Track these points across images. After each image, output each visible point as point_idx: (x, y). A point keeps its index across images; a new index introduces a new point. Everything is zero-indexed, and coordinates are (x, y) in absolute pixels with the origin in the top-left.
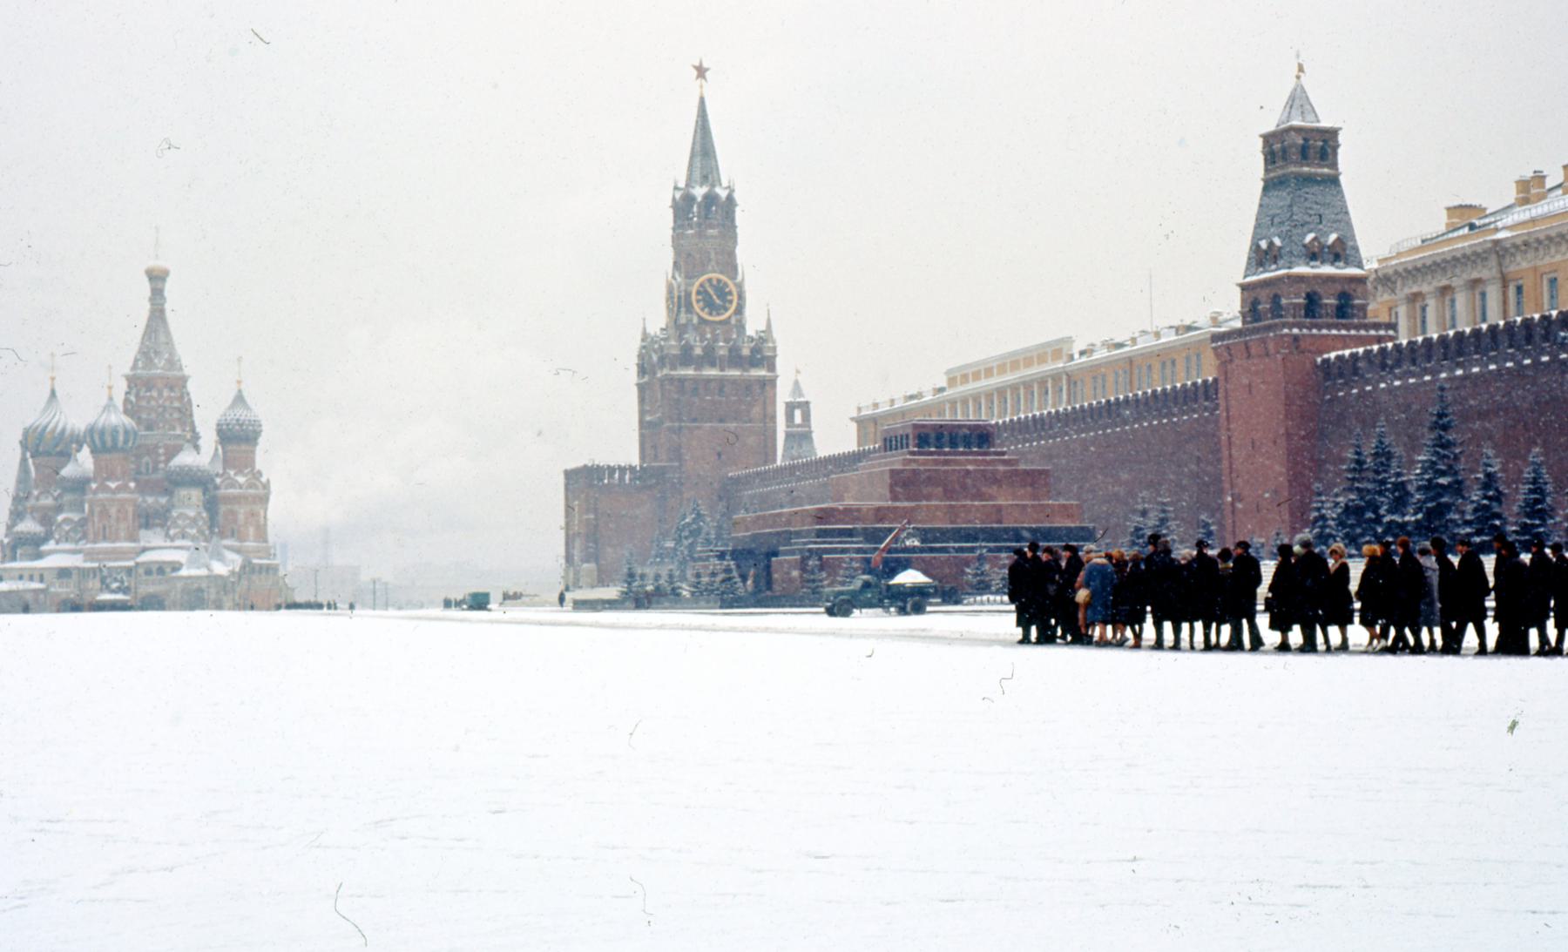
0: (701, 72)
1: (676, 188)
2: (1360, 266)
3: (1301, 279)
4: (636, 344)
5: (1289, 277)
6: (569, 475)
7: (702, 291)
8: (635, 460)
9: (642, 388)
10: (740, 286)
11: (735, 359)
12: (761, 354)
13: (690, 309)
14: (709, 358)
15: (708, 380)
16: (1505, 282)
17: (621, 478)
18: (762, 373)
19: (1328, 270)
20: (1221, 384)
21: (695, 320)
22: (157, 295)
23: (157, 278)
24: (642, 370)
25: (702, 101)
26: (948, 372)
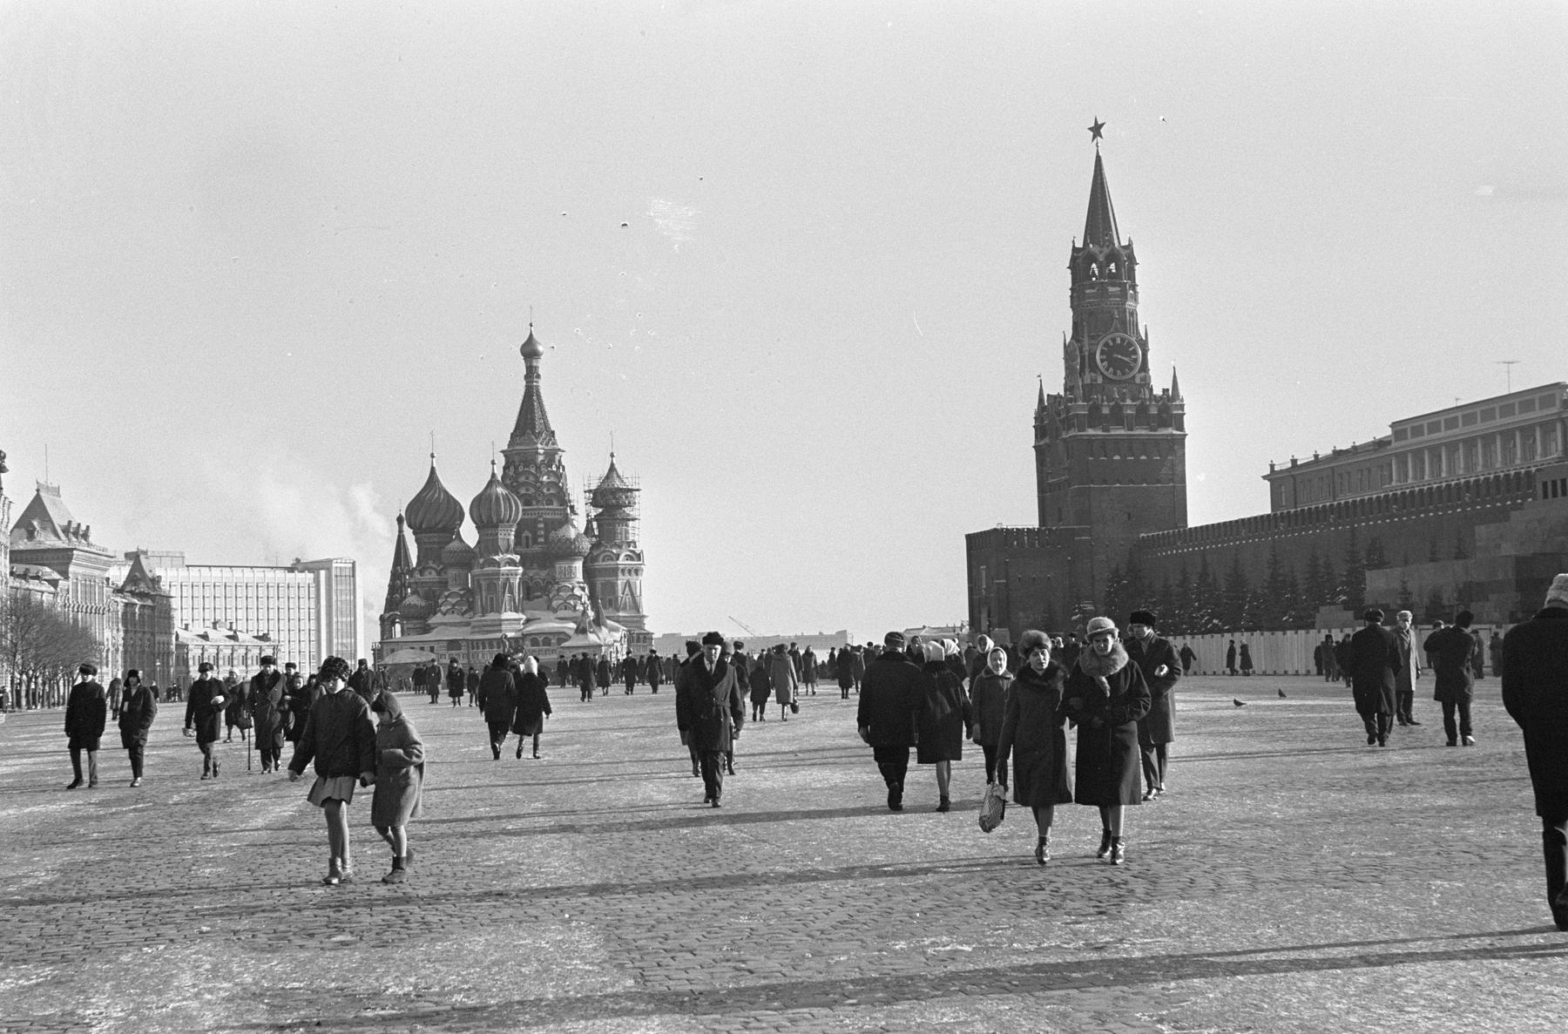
0: (1096, 130)
1: (1075, 249)
6: (971, 539)
7: (1108, 352)
10: (1144, 344)
11: (1142, 416)
12: (1168, 411)
14: (1117, 417)
15: (1117, 440)
21: (1100, 380)
22: (531, 374)
23: (530, 352)
24: (1041, 430)
25: (1098, 159)
26: (1393, 425)
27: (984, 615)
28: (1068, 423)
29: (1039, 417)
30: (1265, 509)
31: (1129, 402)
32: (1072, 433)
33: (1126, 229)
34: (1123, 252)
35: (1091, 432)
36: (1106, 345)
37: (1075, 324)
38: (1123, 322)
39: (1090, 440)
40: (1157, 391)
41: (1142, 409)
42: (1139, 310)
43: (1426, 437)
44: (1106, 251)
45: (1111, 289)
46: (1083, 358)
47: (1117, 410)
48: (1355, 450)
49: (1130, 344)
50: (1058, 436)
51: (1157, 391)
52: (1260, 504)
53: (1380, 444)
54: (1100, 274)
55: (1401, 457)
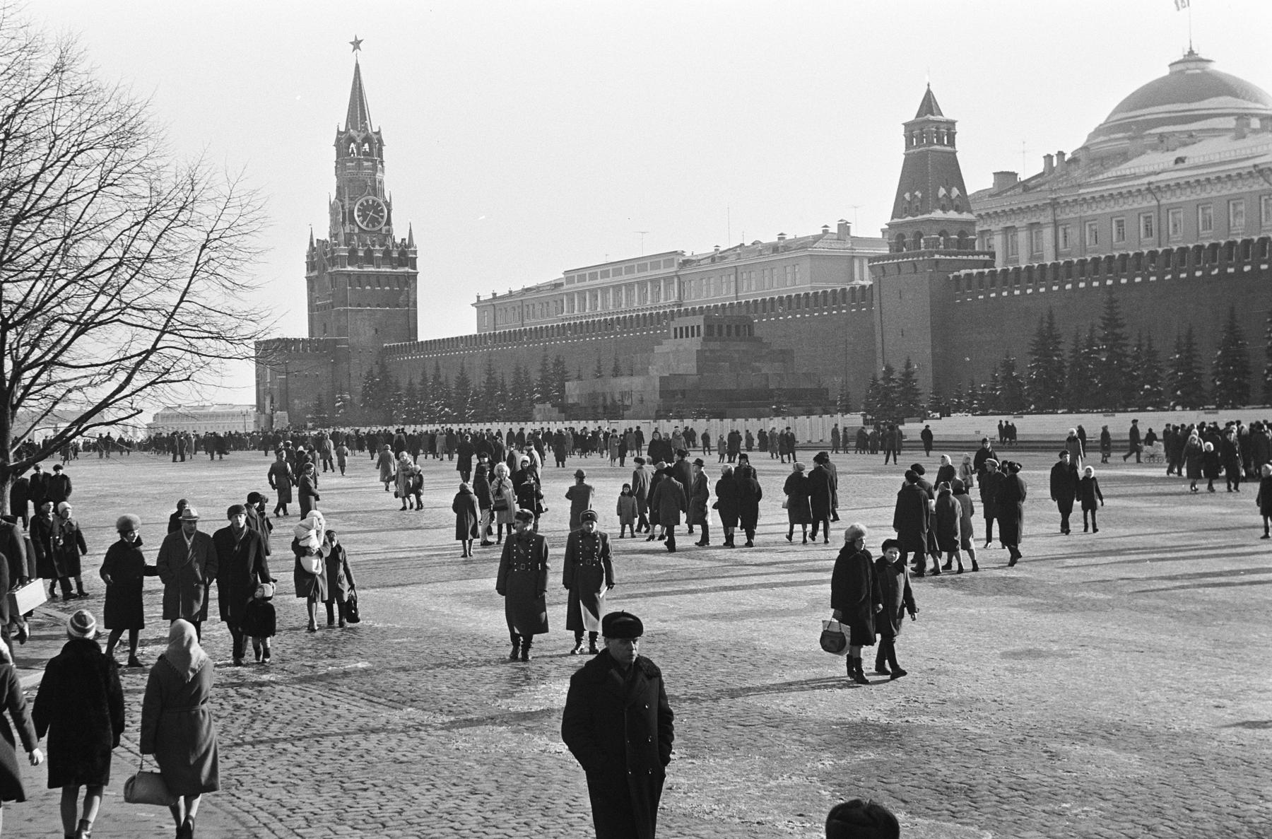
0: (356, 44)
1: (339, 132)
2: (970, 212)
3: (937, 221)
4: (307, 247)
5: (929, 220)
7: (364, 211)
8: (306, 335)
9: (309, 279)
10: (388, 205)
12: (405, 256)
13: (353, 221)
14: (369, 258)
15: (368, 275)
16: (1056, 224)
17: (304, 349)
18: (407, 269)
19: (952, 214)
20: (876, 290)
21: (357, 230)
24: (311, 266)
27: (268, 402)
28: (334, 261)
29: (310, 256)
30: (471, 329)
31: (377, 247)
32: (335, 269)
33: (376, 121)
34: (375, 137)
35: (349, 268)
36: (362, 204)
37: (338, 188)
38: (374, 189)
39: (349, 275)
40: (398, 241)
41: (387, 253)
42: (385, 179)
43: (588, 283)
44: (363, 135)
45: (366, 164)
46: (344, 213)
47: (369, 253)
48: (538, 289)
49: (379, 205)
50: (325, 269)
51: (398, 241)
52: (468, 327)
53: (557, 285)
54: (359, 151)
55: (571, 296)
